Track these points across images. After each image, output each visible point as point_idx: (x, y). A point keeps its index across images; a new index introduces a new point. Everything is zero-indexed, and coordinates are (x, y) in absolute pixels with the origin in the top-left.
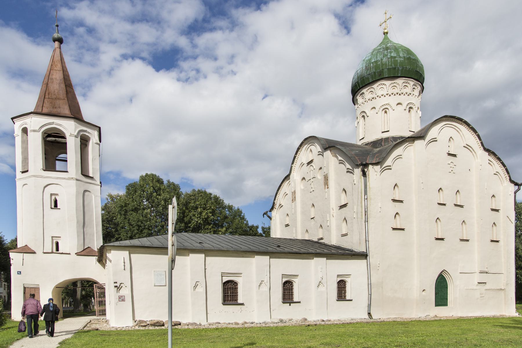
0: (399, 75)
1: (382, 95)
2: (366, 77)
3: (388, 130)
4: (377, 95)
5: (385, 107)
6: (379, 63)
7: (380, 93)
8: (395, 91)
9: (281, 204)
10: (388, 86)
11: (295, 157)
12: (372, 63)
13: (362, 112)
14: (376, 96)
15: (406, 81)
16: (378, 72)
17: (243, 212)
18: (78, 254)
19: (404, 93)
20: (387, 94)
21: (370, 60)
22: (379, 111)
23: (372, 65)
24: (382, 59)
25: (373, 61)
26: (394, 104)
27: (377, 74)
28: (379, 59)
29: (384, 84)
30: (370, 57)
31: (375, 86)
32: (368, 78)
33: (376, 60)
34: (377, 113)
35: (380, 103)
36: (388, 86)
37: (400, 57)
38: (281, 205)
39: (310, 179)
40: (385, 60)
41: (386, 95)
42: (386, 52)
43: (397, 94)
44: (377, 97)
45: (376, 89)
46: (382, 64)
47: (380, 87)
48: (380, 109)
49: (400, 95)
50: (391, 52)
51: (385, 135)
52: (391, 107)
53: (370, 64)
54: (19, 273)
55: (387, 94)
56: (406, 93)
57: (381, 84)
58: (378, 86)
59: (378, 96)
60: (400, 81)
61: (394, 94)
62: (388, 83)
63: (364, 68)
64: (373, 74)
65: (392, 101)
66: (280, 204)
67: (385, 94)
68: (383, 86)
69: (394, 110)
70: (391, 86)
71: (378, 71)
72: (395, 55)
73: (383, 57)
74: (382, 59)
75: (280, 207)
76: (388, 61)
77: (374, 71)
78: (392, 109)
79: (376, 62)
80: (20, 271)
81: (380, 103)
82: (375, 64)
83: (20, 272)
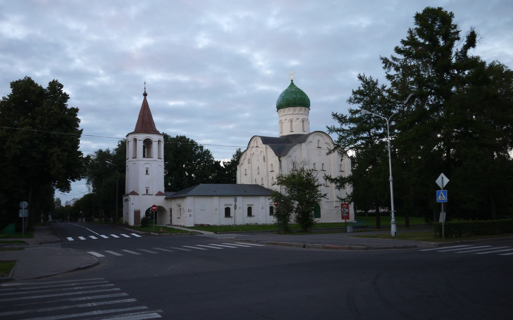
5: (291, 120)
6: (288, 99)
11: (249, 142)
12: (285, 99)
17: (211, 152)
18: (156, 195)
19: (300, 114)
21: (284, 97)
23: (285, 100)
24: (289, 98)
25: (285, 98)
28: (288, 97)
31: (287, 109)
35: (289, 117)
37: (297, 98)
42: (291, 94)
47: (289, 110)
49: (298, 114)
50: (293, 95)
51: (292, 133)
54: (133, 204)
55: (292, 114)
60: (298, 108)
62: (292, 109)
65: (295, 117)
67: (291, 114)
68: (291, 110)
72: (295, 97)
74: (289, 98)
79: (287, 99)
81: (289, 117)
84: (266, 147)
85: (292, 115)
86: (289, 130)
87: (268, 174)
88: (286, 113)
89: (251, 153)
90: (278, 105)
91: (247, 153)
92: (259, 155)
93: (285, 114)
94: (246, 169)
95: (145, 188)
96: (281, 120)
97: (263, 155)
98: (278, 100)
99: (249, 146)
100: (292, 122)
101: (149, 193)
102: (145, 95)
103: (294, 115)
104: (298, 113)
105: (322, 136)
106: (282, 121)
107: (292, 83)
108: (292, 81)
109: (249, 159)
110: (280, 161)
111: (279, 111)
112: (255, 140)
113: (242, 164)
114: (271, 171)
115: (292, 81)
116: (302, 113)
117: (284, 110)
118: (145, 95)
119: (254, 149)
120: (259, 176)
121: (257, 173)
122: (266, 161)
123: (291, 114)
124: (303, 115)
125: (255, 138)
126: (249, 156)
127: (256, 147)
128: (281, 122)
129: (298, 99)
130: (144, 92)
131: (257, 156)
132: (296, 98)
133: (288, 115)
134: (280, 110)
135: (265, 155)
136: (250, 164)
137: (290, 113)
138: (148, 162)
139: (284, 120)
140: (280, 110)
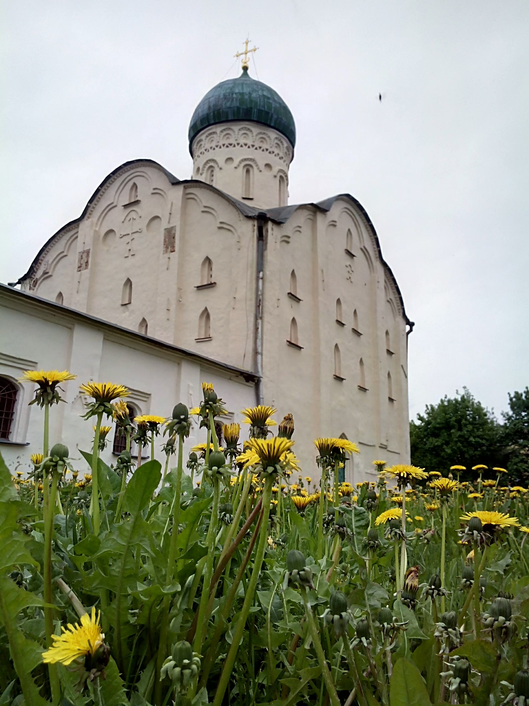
0: (272, 124)
1: (246, 145)
2: (224, 110)
3: (251, 197)
4: (238, 142)
7: (242, 141)
8: (264, 146)
9: (47, 273)
12: (236, 94)
13: (207, 162)
14: (235, 143)
15: (280, 138)
16: (243, 109)
20: (253, 146)
22: (239, 165)
23: (234, 96)
24: (250, 94)
25: (237, 91)
26: (261, 164)
27: (241, 112)
30: (231, 86)
31: (236, 127)
32: (227, 114)
33: (241, 91)
34: (236, 168)
36: (255, 134)
37: (275, 101)
38: (47, 275)
39: (129, 234)
40: (254, 95)
41: (251, 146)
43: (267, 150)
44: (236, 145)
45: (236, 133)
46: (251, 101)
48: (240, 163)
49: (270, 153)
50: (263, 90)
52: (257, 165)
53: (232, 94)
55: (253, 146)
56: (278, 154)
57: (246, 128)
58: (240, 130)
59: (238, 144)
60: (273, 134)
61: (262, 149)
62: (255, 130)
63: (222, 97)
64: (236, 109)
65: (261, 158)
66: (47, 271)
67: (250, 143)
69: (261, 171)
71: (245, 107)
72: (269, 96)
73: (253, 91)
75: (43, 278)
76: (260, 100)
77: (238, 105)
78: (258, 169)
79: (242, 94)
82: (240, 97)
84: (185, 194)
85: (252, 149)
87: (181, 297)
88: (232, 141)
90: (206, 112)
92: (135, 236)
93: (227, 142)
97: (164, 225)
98: (199, 107)
99: (92, 205)
100: (248, 171)
103: (260, 151)
104: (270, 150)
105: (356, 225)
106: (212, 164)
108: (245, 69)
109: (88, 252)
110: (261, 237)
111: (202, 136)
112: (124, 184)
113: (45, 273)
114: (199, 288)
115: (245, 69)
116: (281, 155)
117: (224, 130)
119: (118, 214)
120: (127, 313)
121: (120, 303)
122: (177, 248)
123: (250, 143)
124: (282, 161)
125: (132, 171)
126: (89, 241)
127: (126, 206)
128: (211, 167)
129: (278, 105)
131: (127, 239)
132: (271, 101)
133: (238, 147)
134: (214, 130)
135: (176, 222)
137: (245, 141)
139: (221, 161)
140: (214, 130)
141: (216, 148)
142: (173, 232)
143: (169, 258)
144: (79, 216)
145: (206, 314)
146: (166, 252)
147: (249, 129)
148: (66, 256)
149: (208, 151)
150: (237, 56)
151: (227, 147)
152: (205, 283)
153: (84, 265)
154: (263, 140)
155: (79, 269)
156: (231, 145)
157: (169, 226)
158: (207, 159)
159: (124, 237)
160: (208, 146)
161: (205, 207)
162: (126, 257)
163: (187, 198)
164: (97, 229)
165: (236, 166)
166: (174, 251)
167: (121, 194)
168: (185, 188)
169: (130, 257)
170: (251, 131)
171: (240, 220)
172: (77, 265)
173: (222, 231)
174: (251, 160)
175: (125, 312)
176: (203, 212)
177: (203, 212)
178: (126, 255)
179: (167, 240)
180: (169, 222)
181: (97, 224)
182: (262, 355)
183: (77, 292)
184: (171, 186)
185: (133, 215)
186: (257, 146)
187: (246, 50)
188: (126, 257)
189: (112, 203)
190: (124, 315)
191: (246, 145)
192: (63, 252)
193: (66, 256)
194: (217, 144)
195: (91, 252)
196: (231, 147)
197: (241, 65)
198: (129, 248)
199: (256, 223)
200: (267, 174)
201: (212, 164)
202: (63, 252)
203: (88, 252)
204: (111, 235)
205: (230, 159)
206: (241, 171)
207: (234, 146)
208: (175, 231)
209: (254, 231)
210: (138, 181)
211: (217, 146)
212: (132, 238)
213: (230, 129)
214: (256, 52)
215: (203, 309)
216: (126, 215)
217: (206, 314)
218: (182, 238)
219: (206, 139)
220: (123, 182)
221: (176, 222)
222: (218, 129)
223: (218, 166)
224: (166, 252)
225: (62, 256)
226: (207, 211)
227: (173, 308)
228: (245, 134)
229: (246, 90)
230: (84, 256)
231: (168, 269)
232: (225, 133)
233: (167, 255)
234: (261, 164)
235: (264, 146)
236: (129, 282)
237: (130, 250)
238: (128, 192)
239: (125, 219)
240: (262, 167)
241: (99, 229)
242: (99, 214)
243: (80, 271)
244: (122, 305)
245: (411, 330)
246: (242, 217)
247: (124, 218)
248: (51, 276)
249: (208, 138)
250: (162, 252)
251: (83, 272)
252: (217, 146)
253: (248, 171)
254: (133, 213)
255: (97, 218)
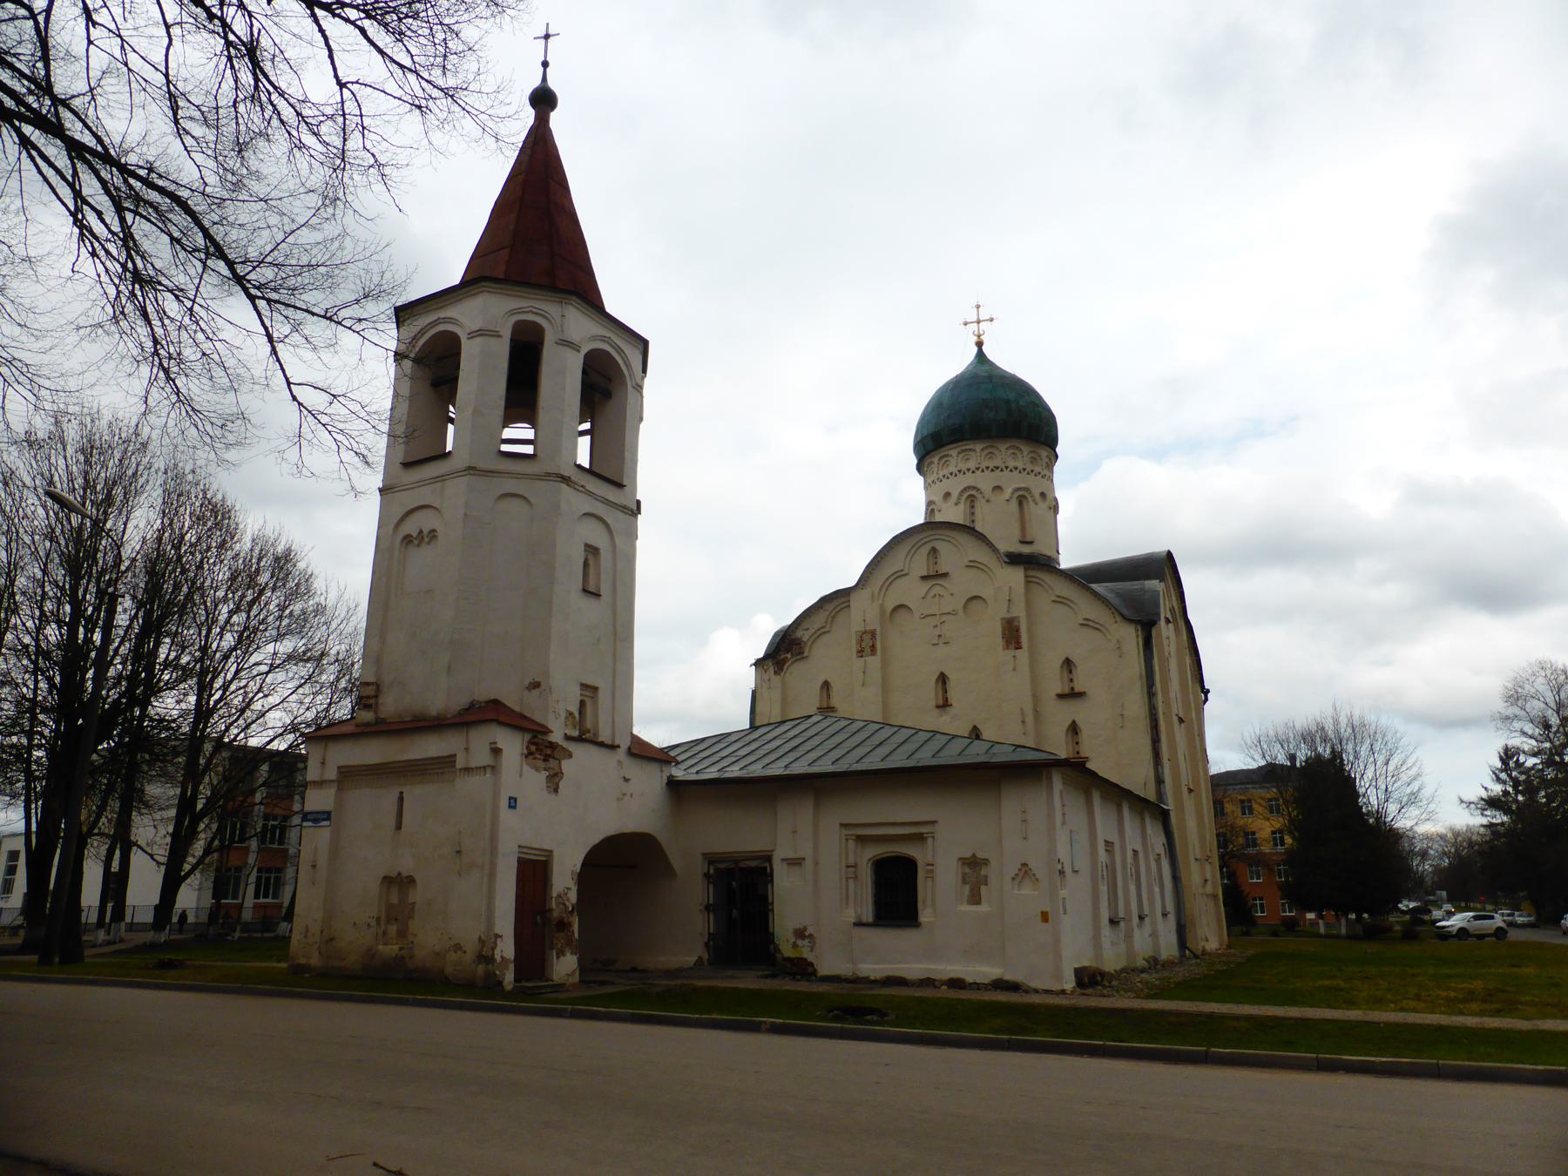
0: (1043, 439)
3: (1028, 539)
5: (1021, 493)
7: (1011, 464)
8: (1037, 469)
10: (1025, 454)
13: (965, 489)
14: (1003, 466)
29: (1017, 448)
34: (1008, 500)
36: (1025, 454)
48: (1013, 494)
49: (1042, 477)
51: (1026, 549)
55: (1024, 470)
58: (1007, 449)
59: (1007, 467)
60: (1044, 453)
67: (1021, 466)
68: (1017, 452)
70: (1030, 456)
78: (1034, 500)
79: (1008, 402)
80: (514, 796)
81: (1012, 482)
83: (515, 800)
84: (1026, 577)
86: (1016, 533)
88: (997, 462)
89: (882, 607)
91: (852, 604)
92: (944, 618)
93: (991, 464)
94: (826, 685)
95: (577, 690)
96: (969, 487)
101: (596, 734)
102: (543, 100)
104: (1043, 473)
106: (973, 492)
107: (981, 356)
108: (980, 344)
109: (873, 634)
114: (1061, 696)
115: (980, 344)
117: (986, 447)
118: (543, 100)
123: (1021, 466)
127: (924, 578)
128: (970, 496)
130: (537, 82)
131: (934, 621)
133: (1006, 472)
134: (971, 447)
136: (874, 662)
137: (1016, 464)
138: (600, 509)
140: (971, 447)
141: (976, 472)
142: (1016, 623)
143: (1014, 657)
144: (852, 583)
145: (1074, 729)
146: (1007, 647)
147: (1017, 448)
148: (828, 632)
149: (964, 473)
150: (966, 325)
151: (992, 470)
152: (1067, 691)
153: (868, 650)
154: (1033, 460)
155: (860, 654)
156: (997, 468)
157: (1007, 616)
158: (965, 486)
159: (929, 619)
160: (963, 466)
161: (1059, 596)
162: (934, 645)
163: (1028, 582)
164: (880, 602)
165: (1007, 497)
166: (1021, 648)
167: (913, 560)
168: (1026, 569)
169: (941, 645)
170: (1021, 450)
171: (1116, 622)
172: (854, 647)
173: (1084, 630)
174: (1027, 489)
175: (942, 716)
176: (1054, 601)
177: (1054, 601)
178: (936, 642)
179: (1007, 632)
180: (1008, 611)
181: (879, 594)
182: (1164, 782)
183: (863, 685)
184: (1003, 564)
185: (937, 590)
186: (1028, 470)
187: (978, 319)
188: (934, 645)
189: (902, 571)
190: (943, 718)
191: (1016, 468)
192: (824, 627)
193: (828, 632)
194: (977, 466)
195: (878, 633)
196: (997, 472)
197: (975, 339)
198: (938, 633)
199: (1139, 628)
200: (1043, 506)
201: (973, 492)
202: (824, 627)
203: (873, 634)
204: (902, 614)
205: (998, 488)
206: (1014, 504)
207: (1002, 470)
208: (1019, 622)
209: (1137, 637)
210: (940, 546)
211: (978, 469)
212: (942, 621)
213: (992, 446)
214: (993, 323)
215: (1070, 722)
216: (927, 589)
217: (1074, 729)
218: (1029, 631)
219: (957, 456)
220: (915, 545)
221: (1019, 611)
222: (979, 447)
223: (984, 497)
224: (1007, 647)
225: (821, 633)
226: (1060, 601)
227: (1030, 718)
228: (1013, 453)
229: (1012, 396)
230: (867, 638)
231: (1014, 669)
232: (987, 451)
233: (1011, 652)
234: (1037, 494)
235: (1037, 469)
236: (943, 679)
237: (940, 636)
238: (925, 558)
239: (926, 594)
240: (1037, 496)
241: (883, 601)
242: (881, 583)
243: (862, 656)
244: (938, 707)
245: (1206, 699)
246: (1118, 618)
247: (924, 592)
248: (807, 657)
249: (962, 455)
250: (1001, 647)
251: (870, 659)
252: (978, 469)
253: (1020, 504)
254: (938, 588)
255: (878, 588)
